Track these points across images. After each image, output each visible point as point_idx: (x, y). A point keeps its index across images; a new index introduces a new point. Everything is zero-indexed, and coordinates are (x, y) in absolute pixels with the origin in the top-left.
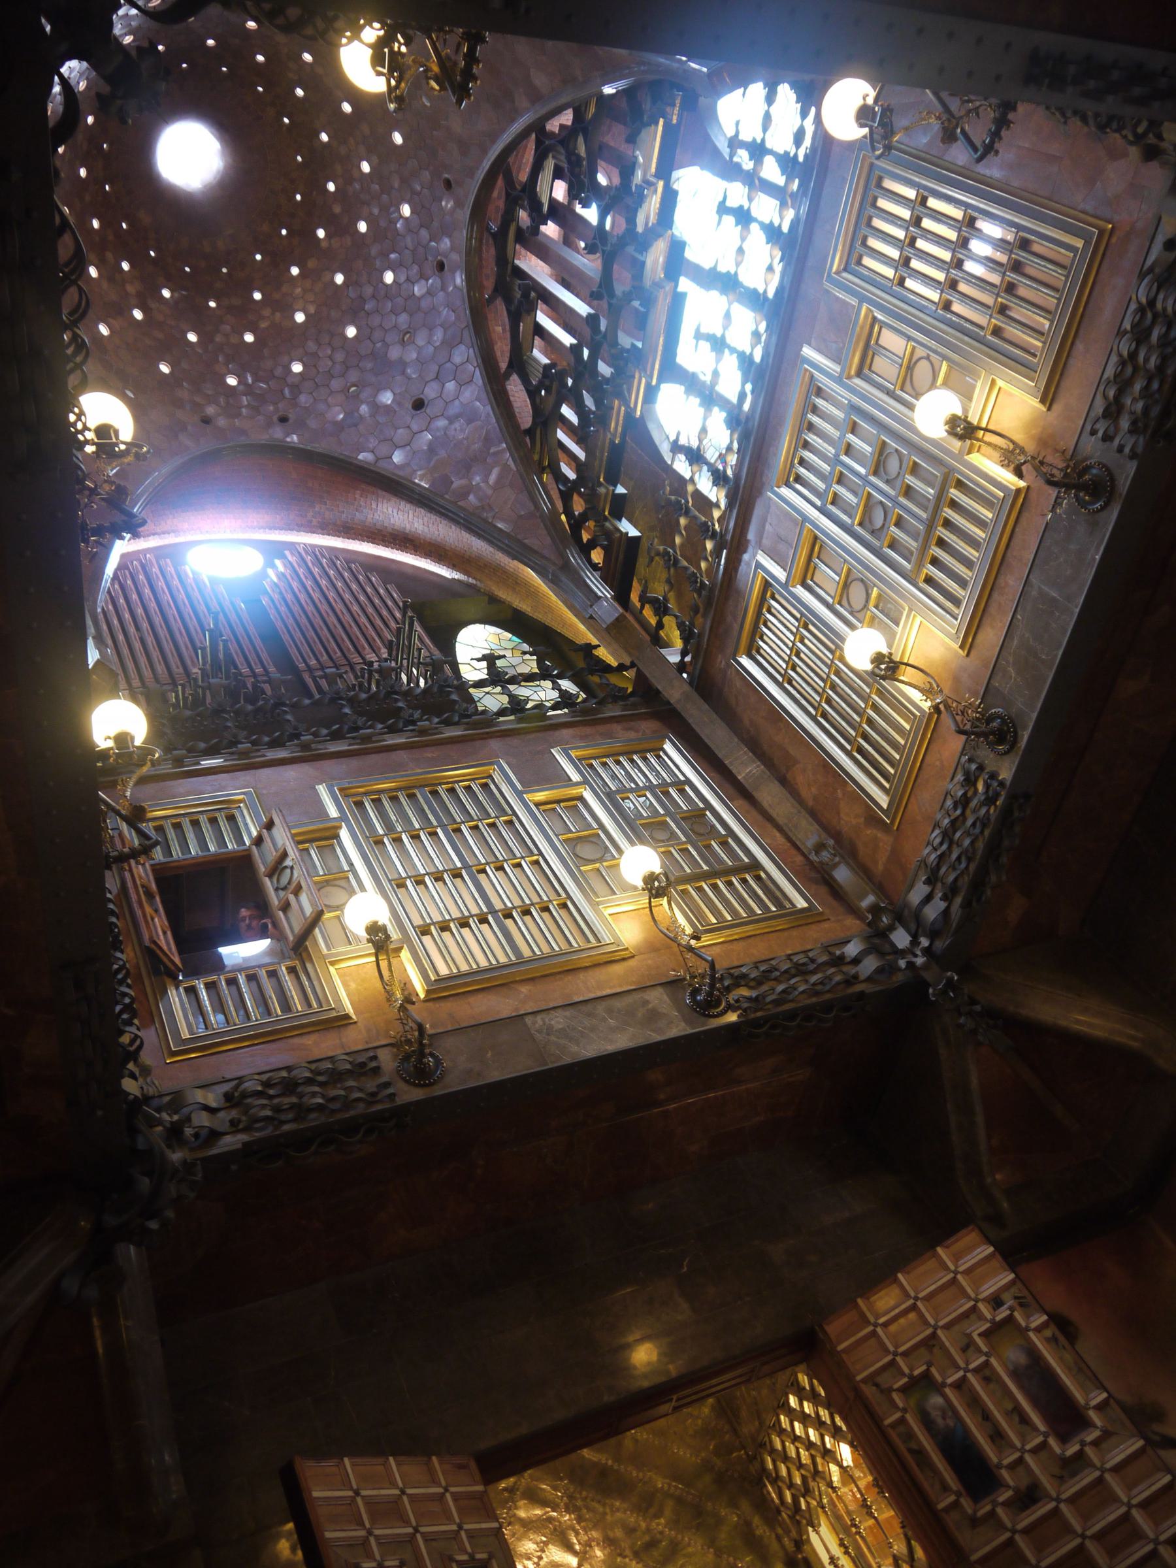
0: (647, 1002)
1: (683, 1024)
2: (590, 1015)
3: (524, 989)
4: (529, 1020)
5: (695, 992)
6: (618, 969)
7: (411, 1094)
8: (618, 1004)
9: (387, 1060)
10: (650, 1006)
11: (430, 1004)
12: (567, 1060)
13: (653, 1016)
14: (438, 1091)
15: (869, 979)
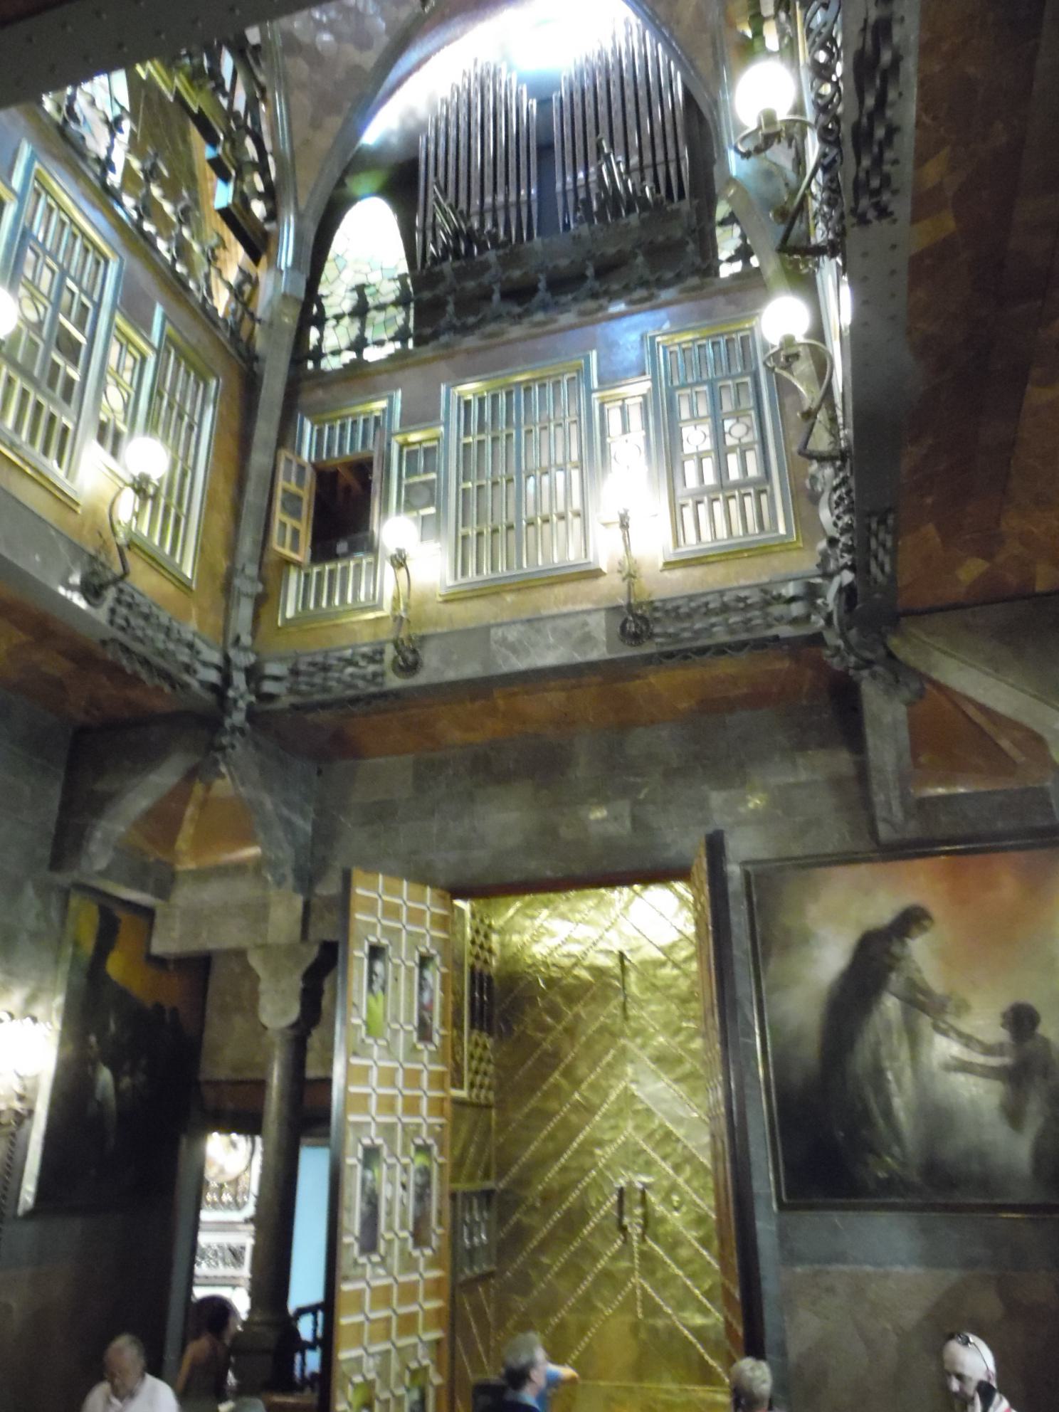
0: (585, 624)
1: (605, 649)
2: (538, 631)
3: (509, 598)
4: (493, 631)
5: (626, 621)
6: (585, 587)
7: (394, 682)
8: (561, 623)
9: (390, 652)
10: (587, 629)
11: (442, 606)
12: (505, 669)
13: (587, 639)
14: (421, 679)
15: (795, 621)
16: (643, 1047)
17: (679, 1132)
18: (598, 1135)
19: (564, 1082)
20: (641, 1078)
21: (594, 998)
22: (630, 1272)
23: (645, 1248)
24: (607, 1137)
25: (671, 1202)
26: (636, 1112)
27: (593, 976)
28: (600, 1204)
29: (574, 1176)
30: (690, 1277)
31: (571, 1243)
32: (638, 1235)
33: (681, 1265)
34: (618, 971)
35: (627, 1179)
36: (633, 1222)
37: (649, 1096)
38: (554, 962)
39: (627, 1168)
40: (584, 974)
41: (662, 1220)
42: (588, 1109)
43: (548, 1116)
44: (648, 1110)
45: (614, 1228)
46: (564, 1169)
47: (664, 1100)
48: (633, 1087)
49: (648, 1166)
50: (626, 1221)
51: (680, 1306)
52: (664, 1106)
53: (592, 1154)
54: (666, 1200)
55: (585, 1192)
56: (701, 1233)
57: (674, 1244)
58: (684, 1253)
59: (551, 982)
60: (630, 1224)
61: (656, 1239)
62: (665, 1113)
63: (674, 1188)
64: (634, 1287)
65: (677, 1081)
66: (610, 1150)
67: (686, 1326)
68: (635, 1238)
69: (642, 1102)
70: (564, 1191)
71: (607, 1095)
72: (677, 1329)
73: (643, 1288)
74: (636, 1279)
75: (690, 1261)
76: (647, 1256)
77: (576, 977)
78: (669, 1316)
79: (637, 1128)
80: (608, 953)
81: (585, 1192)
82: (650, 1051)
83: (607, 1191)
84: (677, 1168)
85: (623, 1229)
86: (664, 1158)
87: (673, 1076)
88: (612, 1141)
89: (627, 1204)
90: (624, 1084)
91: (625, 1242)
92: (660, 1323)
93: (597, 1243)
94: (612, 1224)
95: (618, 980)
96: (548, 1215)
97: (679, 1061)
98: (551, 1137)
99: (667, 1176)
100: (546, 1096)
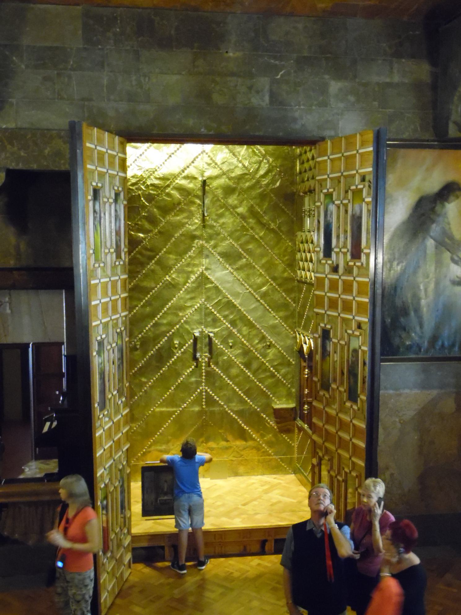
16: (215, 247)
17: (236, 302)
18: (182, 302)
19: (158, 268)
20: (213, 267)
21: (182, 211)
22: (199, 383)
23: (209, 369)
24: (188, 304)
25: (228, 343)
26: (208, 289)
27: (181, 195)
28: (181, 346)
29: (164, 329)
30: (236, 384)
31: (161, 369)
32: (205, 362)
33: (230, 378)
34: (200, 193)
35: (200, 330)
36: (203, 356)
37: (217, 279)
38: (152, 182)
39: (200, 323)
40: (176, 194)
41: (222, 353)
42: (174, 286)
43: (147, 291)
44: (216, 288)
45: (190, 359)
46: (156, 325)
47: (228, 282)
48: (207, 273)
49: (215, 321)
50: (198, 355)
51: (229, 401)
52: (228, 285)
53: (177, 315)
54: (224, 341)
55: (171, 339)
56: (246, 360)
57: (227, 366)
58: (234, 371)
59: (150, 198)
60: (201, 356)
61: (216, 364)
62: (227, 290)
63: (230, 335)
64: (201, 392)
65: (237, 269)
66: (190, 311)
67: (232, 411)
68: (204, 364)
69: (212, 283)
70: (156, 339)
71: (188, 278)
72: (227, 412)
73: (206, 391)
74: (203, 387)
75: (237, 376)
76: (210, 375)
77: (168, 195)
78: (222, 406)
79: (208, 299)
80: (192, 178)
81: (171, 339)
82: (219, 249)
83: (186, 337)
84: (233, 323)
85: (195, 359)
86: (225, 317)
87: (235, 267)
88: (191, 307)
89: (199, 346)
90: (201, 270)
91: (196, 367)
92: (216, 409)
93: (179, 366)
94: (189, 356)
95: (200, 200)
96: (145, 353)
97: (240, 257)
98: (148, 303)
99: (227, 328)
100: (146, 276)
